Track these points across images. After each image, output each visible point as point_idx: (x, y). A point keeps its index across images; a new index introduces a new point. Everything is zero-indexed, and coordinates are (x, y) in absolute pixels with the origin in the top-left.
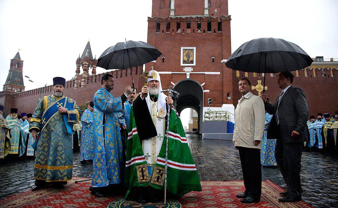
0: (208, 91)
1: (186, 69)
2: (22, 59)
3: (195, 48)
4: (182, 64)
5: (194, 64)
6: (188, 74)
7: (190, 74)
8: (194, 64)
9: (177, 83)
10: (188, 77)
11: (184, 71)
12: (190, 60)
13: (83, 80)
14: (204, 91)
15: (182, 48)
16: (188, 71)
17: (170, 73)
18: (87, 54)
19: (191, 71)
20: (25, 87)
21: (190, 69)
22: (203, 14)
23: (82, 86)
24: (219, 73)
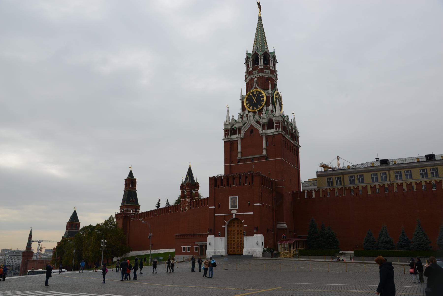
0: (246, 226)
1: (233, 212)
2: (135, 177)
3: (237, 197)
4: (230, 208)
5: (237, 208)
6: (234, 215)
8: (237, 208)
9: (229, 221)
10: (234, 217)
13: (187, 204)
16: (234, 212)
17: (224, 214)
18: (188, 180)
20: (139, 206)
24: (252, 213)
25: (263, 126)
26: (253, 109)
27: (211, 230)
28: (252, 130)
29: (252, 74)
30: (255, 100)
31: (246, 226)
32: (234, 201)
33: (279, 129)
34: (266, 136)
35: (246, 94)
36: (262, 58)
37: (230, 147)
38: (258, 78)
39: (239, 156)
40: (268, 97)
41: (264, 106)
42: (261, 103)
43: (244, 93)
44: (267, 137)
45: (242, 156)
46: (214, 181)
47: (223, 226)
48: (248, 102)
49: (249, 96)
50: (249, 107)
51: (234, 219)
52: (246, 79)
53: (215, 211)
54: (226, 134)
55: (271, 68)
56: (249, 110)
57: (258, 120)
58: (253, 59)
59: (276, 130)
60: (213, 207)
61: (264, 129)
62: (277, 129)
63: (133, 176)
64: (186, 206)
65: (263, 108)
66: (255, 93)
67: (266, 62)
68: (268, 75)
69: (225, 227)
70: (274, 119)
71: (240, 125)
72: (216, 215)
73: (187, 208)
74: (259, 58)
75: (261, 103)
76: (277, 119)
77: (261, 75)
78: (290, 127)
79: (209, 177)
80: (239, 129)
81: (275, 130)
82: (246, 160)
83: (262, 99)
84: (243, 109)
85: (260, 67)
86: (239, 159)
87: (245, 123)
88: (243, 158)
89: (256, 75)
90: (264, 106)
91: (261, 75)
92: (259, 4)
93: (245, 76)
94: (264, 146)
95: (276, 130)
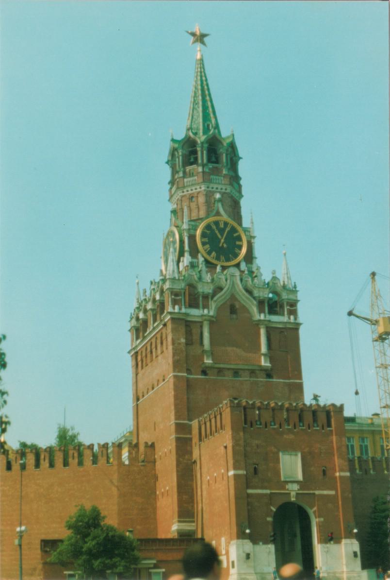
6: (293, 494)
11: (288, 490)
17: (268, 491)
19: (297, 489)
21: (296, 487)
24: (333, 493)
25: (261, 303)
26: (218, 258)
28: (233, 308)
30: (223, 241)
33: (295, 319)
42: (237, 251)
44: (270, 331)
48: (206, 240)
49: (208, 227)
50: (209, 253)
56: (209, 258)
61: (261, 311)
66: (222, 226)
68: (237, 194)
70: (285, 296)
72: (250, 491)
80: (206, 297)
83: (238, 243)
84: (194, 252)
87: (220, 289)
88: (217, 366)
94: (264, 349)
95: (289, 318)
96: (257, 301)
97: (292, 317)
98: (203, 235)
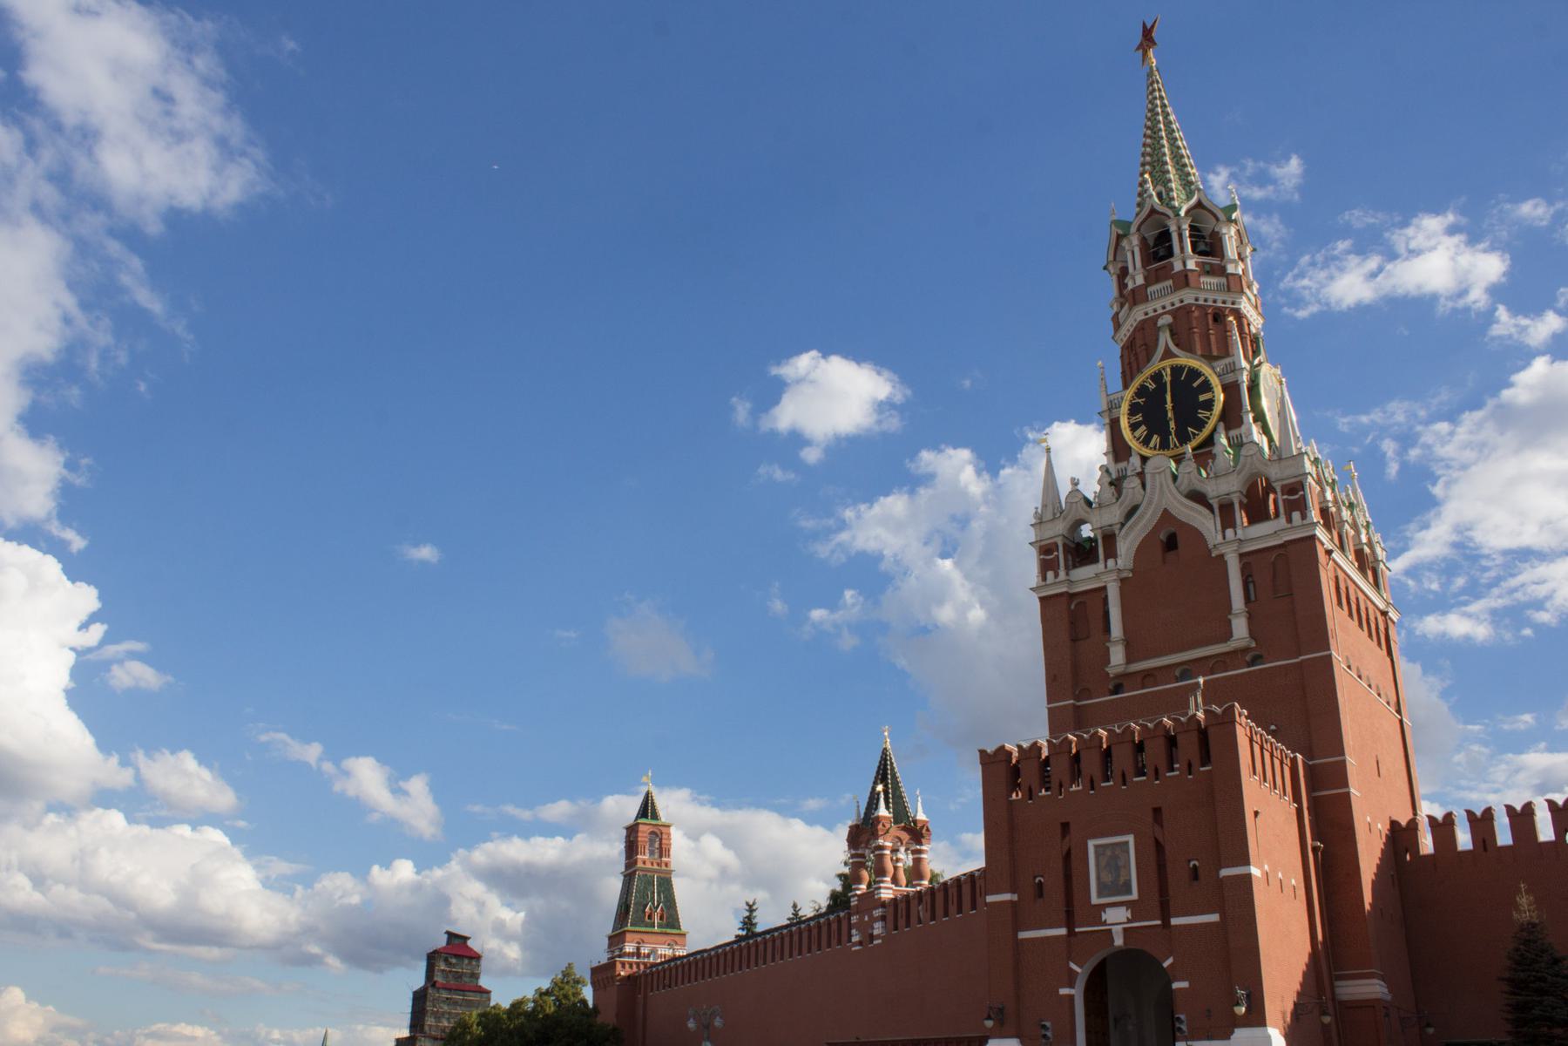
0: (1184, 984)
3: (1130, 839)
4: (1095, 900)
5: (1135, 896)
7: (1125, 930)
8: (1135, 896)
10: (1119, 941)
11: (1105, 923)
12: (1122, 880)
13: (877, 913)
14: (1176, 985)
15: (1091, 844)
16: (1117, 918)
22: (1227, 635)
23: (878, 937)
27: (1001, 1010)
28: (1171, 540)
29: (1146, 300)
30: (1169, 406)
31: (1184, 984)
32: (1112, 858)
33: (1304, 517)
34: (1242, 556)
35: (1126, 387)
36: (1186, 226)
37: (1070, 624)
38: (1175, 313)
39: (1117, 656)
40: (1231, 389)
41: (1215, 430)
42: (1202, 414)
43: (1116, 382)
44: (1248, 561)
45: (1130, 659)
46: (1005, 774)
47: (1063, 991)
48: (1139, 418)
49: (1142, 391)
50: (1146, 442)
51: (1121, 953)
52: (1117, 326)
53: (1017, 917)
54: (1046, 566)
55: (1230, 269)
56: (1146, 452)
57: (1199, 487)
58: (1143, 241)
59: (1289, 520)
60: (1007, 897)
61: (1228, 521)
62: (1296, 515)
63: (655, 816)
64: (873, 920)
65: (1210, 441)
67: (1202, 247)
68: (1220, 298)
69: (1071, 997)
71: (1113, 516)
72: (1023, 935)
73: (878, 929)
74: (1173, 228)
75: (1202, 414)
76: (1289, 472)
77: (1188, 296)
78: (1346, 514)
79: (982, 752)
81: (1283, 519)
82: (1148, 677)
83: (1202, 398)
85: (1178, 267)
86: (1118, 676)
89: (1162, 302)
90: (1215, 430)
91: (1188, 296)
92: (1147, 34)
93: (1115, 318)
95: (1289, 520)
96: (1216, 506)
97: (1296, 515)
98: (1133, 409)
